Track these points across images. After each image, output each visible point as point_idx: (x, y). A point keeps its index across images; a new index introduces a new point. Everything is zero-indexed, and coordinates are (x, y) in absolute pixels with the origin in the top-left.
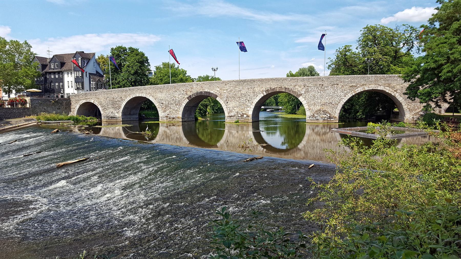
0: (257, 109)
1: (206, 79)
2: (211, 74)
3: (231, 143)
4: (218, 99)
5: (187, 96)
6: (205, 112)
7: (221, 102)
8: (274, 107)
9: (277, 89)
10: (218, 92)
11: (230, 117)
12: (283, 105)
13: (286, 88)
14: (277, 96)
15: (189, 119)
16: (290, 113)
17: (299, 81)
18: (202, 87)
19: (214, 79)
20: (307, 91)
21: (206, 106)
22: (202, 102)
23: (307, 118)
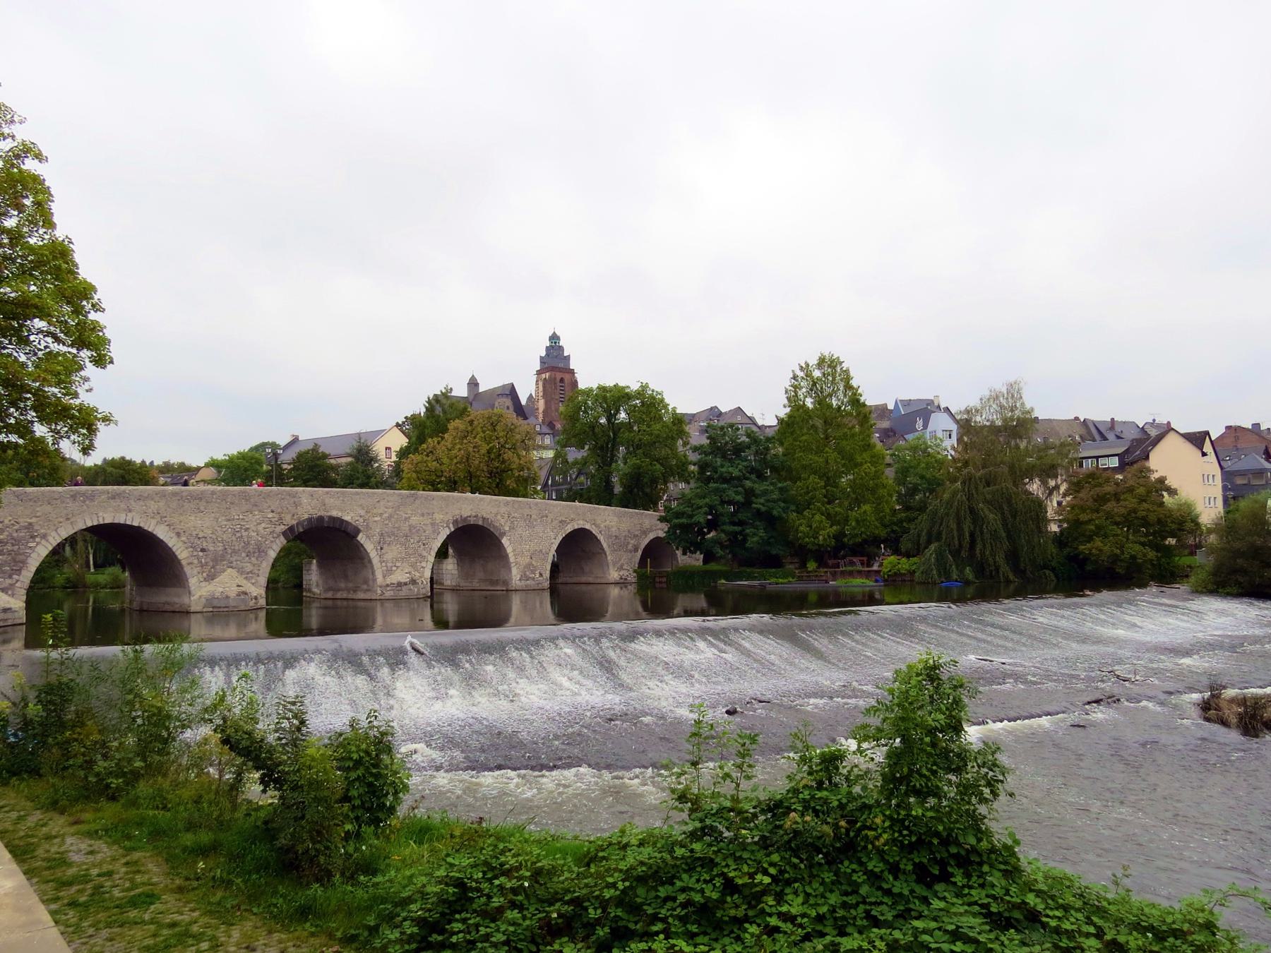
5: (283, 528)
11: (400, 584)
13: (484, 519)
20: (512, 528)
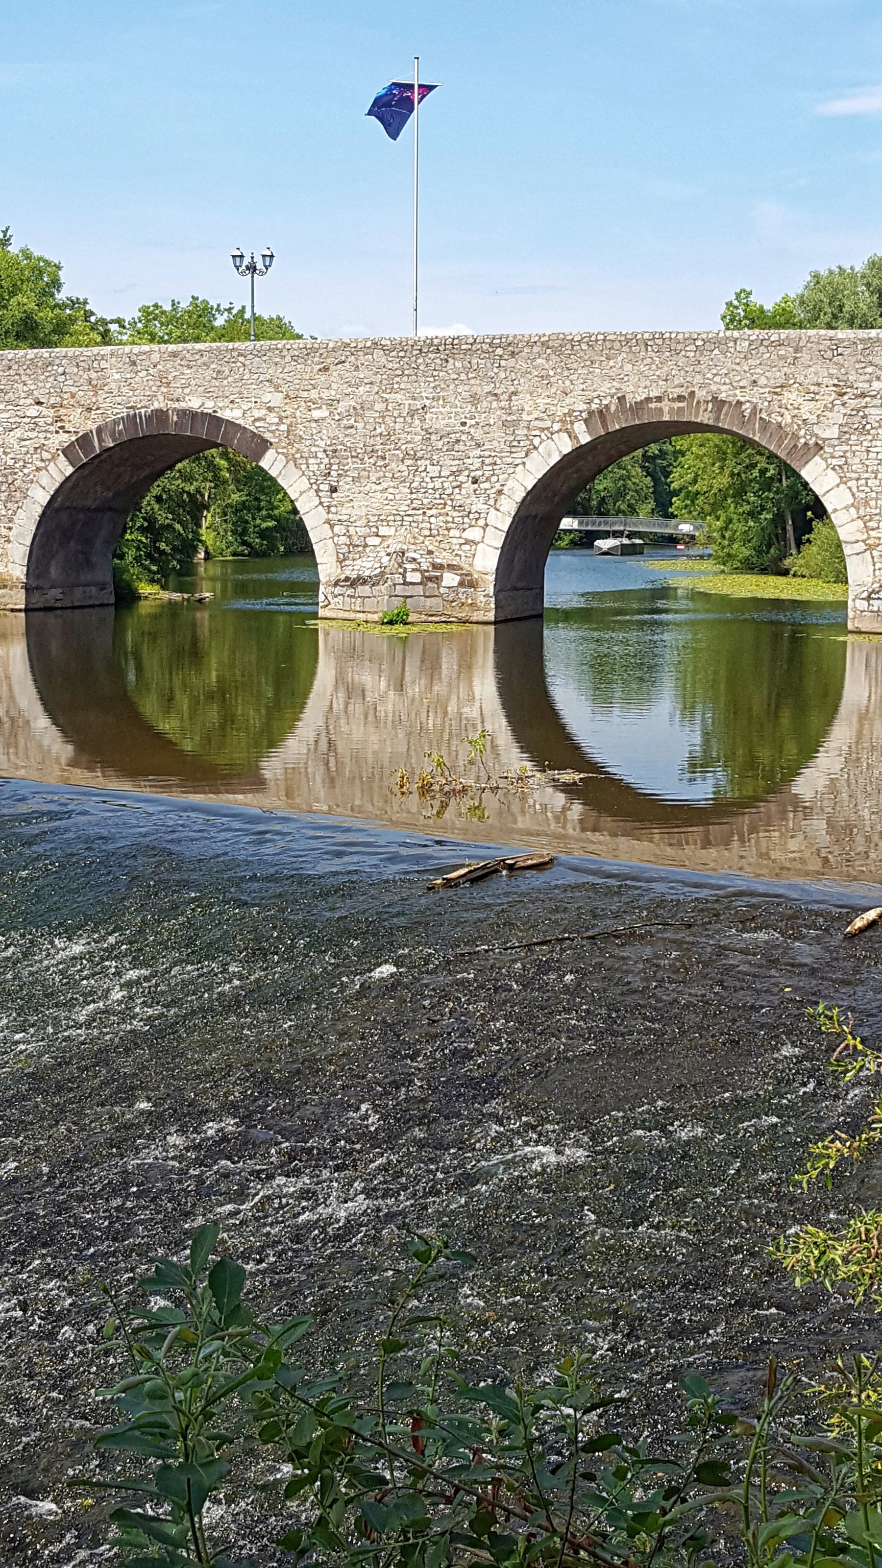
0: (532, 536)
1: (195, 323)
2: (228, 292)
3: (357, 759)
4: (271, 463)
5: (65, 439)
6: (188, 547)
7: (295, 485)
8: (645, 521)
9: (665, 405)
10: (273, 418)
12: (703, 515)
13: (719, 404)
14: (663, 454)
15: (78, 596)
16: (748, 567)
17: (805, 356)
18: (163, 380)
19: (246, 327)
21: (195, 508)
22: (162, 482)
23: (856, 605)
